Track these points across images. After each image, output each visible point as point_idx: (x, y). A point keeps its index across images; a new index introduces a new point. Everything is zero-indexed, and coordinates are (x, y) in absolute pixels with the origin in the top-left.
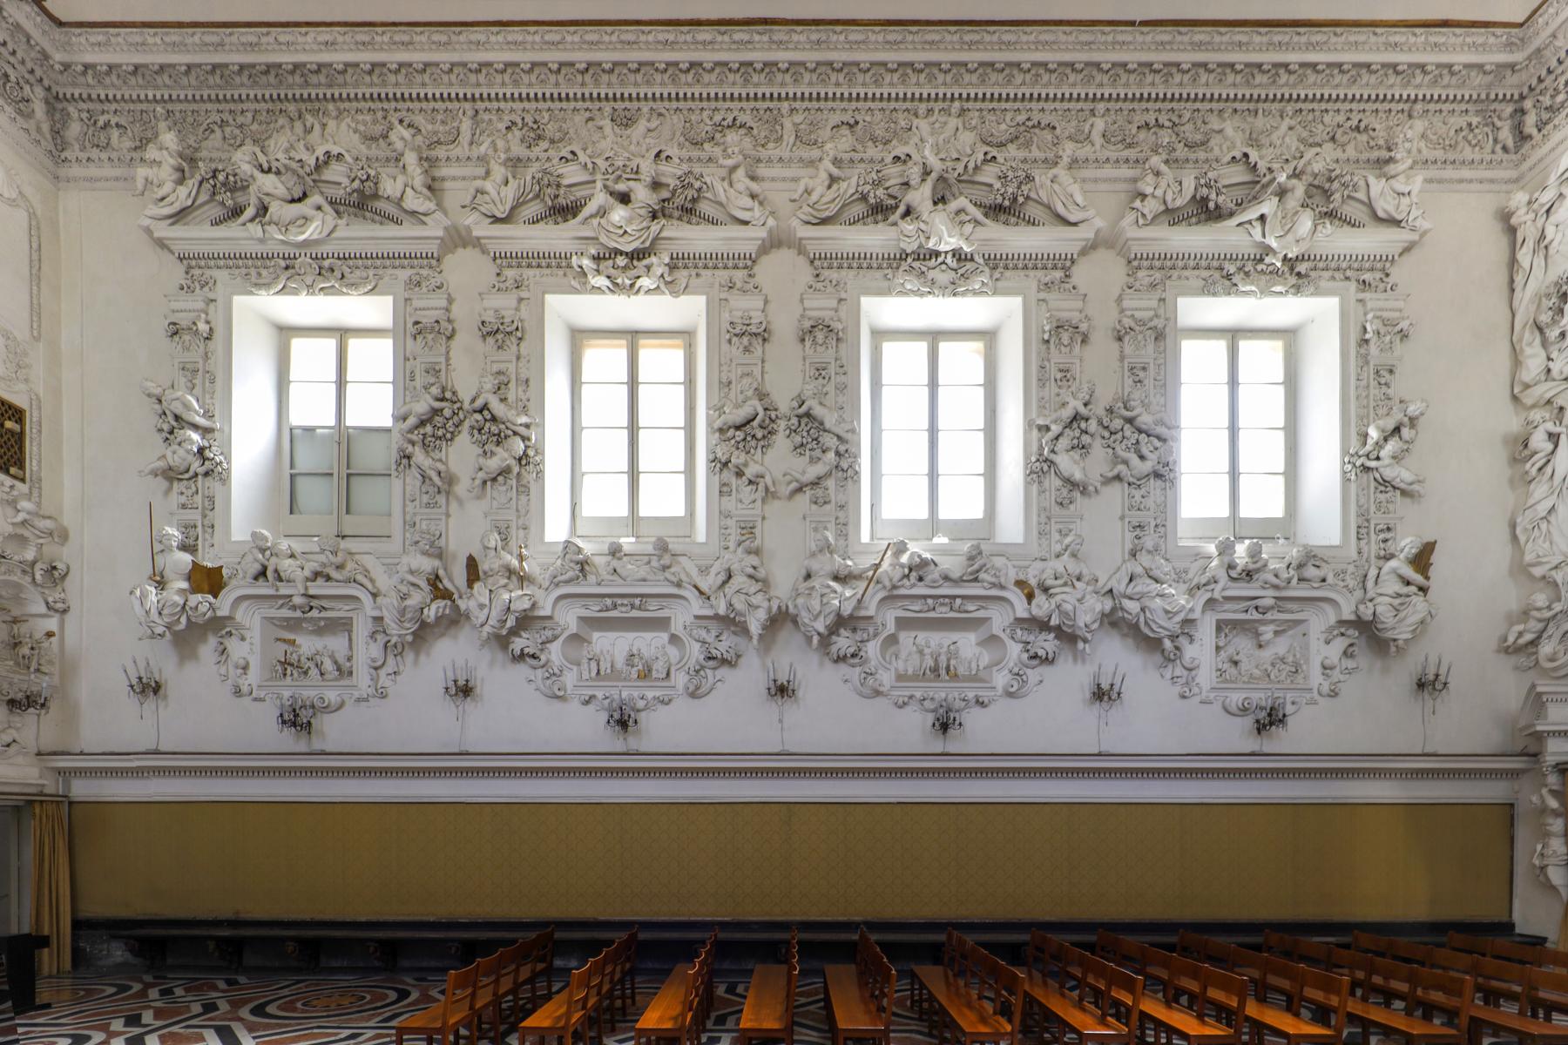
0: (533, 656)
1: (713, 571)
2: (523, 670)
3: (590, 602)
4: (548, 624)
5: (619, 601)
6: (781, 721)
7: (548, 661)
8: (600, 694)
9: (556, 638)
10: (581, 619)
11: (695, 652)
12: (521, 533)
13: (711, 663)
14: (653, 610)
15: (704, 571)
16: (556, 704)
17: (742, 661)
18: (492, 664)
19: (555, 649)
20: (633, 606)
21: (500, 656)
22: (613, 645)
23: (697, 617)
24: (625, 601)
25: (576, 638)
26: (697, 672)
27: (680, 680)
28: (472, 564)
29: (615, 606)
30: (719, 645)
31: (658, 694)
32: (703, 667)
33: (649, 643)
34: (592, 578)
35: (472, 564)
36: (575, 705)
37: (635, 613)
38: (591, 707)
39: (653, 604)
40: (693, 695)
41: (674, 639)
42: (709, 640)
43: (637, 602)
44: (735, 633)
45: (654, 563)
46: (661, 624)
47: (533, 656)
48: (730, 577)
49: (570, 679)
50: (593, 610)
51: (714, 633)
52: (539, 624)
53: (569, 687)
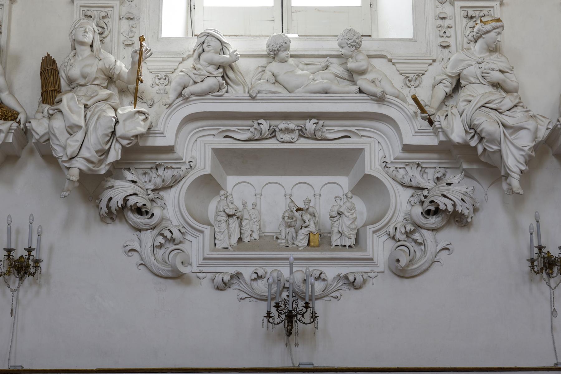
0: (139, 211)
1: (427, 81)
2: (119, 233)
3: (230, 125)
4: (162, 159)
5: (282, 125)
6: (554, 313)
7: (162, 219)
8: (247, 273)
9: (176, 181)
10: (218, 153)
11: (402, 204)
12: (125, 25)
13: (433, 221)
14: (334, 138)
15: (412, 79)
16: (173, 290)
17: (480, 219)
18: (67, 224)
19: (170, 197)
20: (302, 133)
21: (82, 211)
22: (266, 197)
23: (407, 148)
24: (292, 125)
25: (209, 184)
26: (408, 234)
27: (380, 248)
28: (49, 69)
29: (273, 134)
30: (446, 190)
31: (344, 271)
32: (418, 226)
33: (325, 192)
34: (237, 90)
35: (49, 69)
36: (204, 289)
37: (304, 144)
38: (231, 294)
39: (334, 129)
40: (402, 273)
41: (367, 185)
42: (424, 184)
43: (310, 125)
44: (468, 175)
45: (336, 68)
46: (343, 160)
47: (139, 211)
48: (457, 87)
49: (195, 248)
50: (240, 137)
51: (431, 174)
52: (149, 160)
53: (196, 258)
